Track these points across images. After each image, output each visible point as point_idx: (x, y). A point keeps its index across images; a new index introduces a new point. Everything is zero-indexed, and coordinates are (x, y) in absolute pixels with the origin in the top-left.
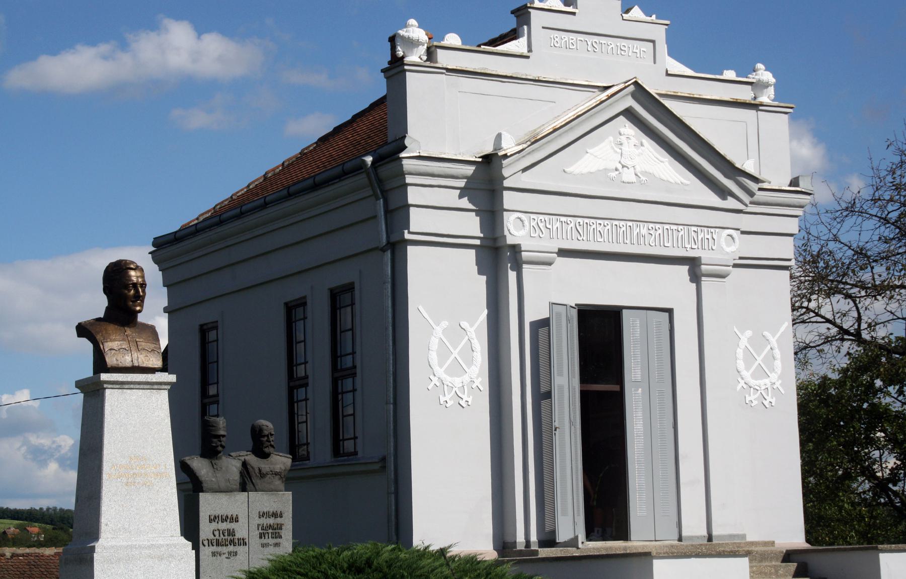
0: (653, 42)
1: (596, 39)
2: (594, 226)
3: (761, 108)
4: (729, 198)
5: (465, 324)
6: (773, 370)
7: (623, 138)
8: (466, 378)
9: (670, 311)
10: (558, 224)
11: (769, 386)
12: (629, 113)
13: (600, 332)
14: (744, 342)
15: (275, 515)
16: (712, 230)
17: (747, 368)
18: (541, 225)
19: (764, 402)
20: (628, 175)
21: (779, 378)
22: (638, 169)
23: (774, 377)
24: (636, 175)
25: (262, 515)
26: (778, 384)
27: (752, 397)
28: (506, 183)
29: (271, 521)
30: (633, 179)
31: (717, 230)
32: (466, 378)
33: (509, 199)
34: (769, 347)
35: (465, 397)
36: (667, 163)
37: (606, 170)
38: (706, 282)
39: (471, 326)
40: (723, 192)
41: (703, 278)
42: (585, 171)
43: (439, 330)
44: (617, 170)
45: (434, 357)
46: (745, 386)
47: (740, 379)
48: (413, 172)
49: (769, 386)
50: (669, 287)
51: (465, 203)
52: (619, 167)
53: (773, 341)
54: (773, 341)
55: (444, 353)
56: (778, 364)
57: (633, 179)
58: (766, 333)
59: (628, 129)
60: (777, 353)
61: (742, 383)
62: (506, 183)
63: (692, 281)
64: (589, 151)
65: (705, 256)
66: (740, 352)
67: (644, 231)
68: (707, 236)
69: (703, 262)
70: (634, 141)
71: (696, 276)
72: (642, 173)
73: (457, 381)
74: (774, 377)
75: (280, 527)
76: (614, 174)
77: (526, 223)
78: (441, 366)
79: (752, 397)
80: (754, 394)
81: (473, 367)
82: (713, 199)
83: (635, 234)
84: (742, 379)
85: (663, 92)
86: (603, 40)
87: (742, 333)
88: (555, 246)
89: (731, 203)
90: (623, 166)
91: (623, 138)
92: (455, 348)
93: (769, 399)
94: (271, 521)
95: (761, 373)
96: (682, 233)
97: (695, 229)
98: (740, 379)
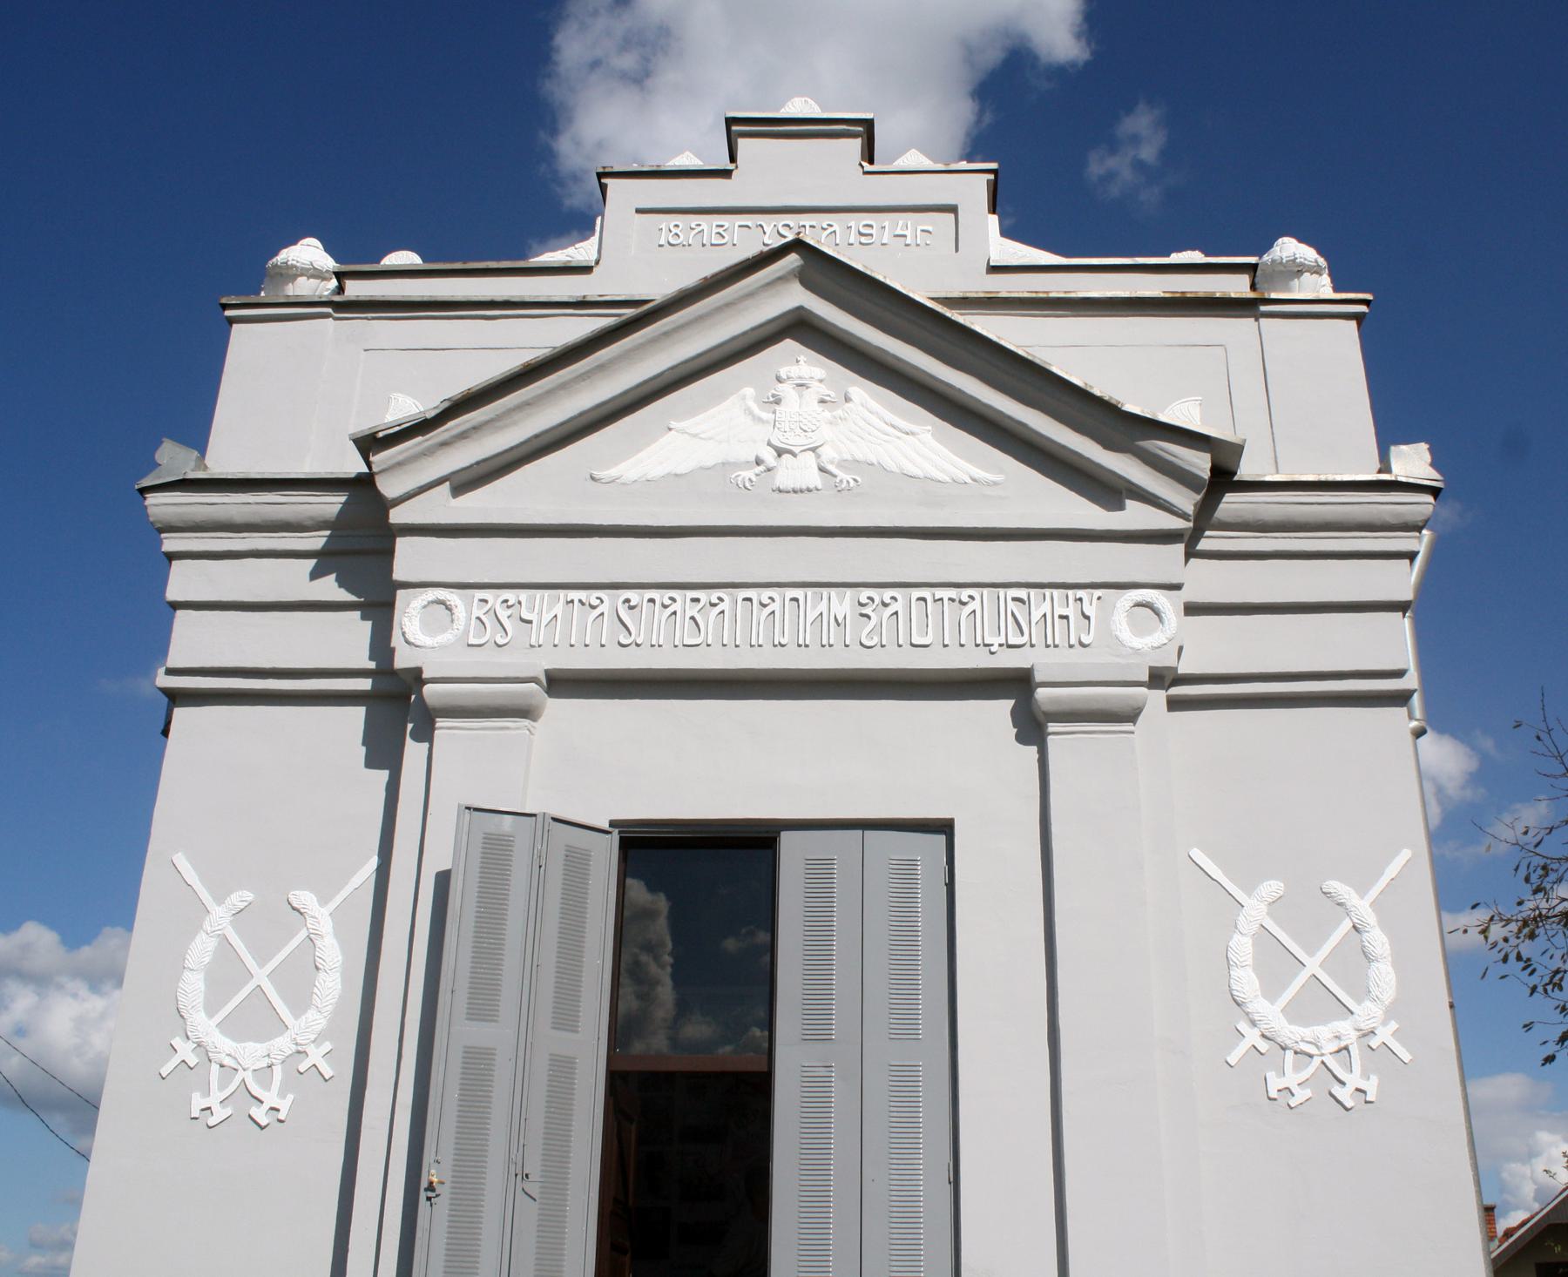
0: (953, 209)
2: (676, 607)
3: (1263, 308)
4: (1129, 503)
5: (305, 898)
7: (786, 390)
8: (282, 1045)
10: (559, 609)
11: (1351, 1038)
13: (702, 893)
14: (1255, 910)
16: (1080, 593)
17: (1271, 990)
18: (503, 614)
20: (798, 472)
21: (1390, 1013)
22: (828, 453)
23: (1368, 1013)
24: (822, 470)
26: (1385, 1034)
27: (1290, 1077)
28: (397, 516)
30: (815, 479)
31: (1098, 593)
32: (282, 1045)
33: (409, 558)
34: (1346, 925)
35: (271, 1098)
36: (928, 437)
38: (1061, 739)
39: (323, 901)
40: (1109, 491)
41: (1052, 727)
42: (656, 471)
43: (220, 916)
44: (758, 462)
45: (193, 987)
46: (1263, 1046)
47: (1243, 1026)
48: (175, 521)
49: (1351, 1038)
50: (954, 758)
51: (329, 588)
52: (769, 456)
53: (1362, 907)
54: (1362, 907)
55: (225, 974)
56: (1384, 977)
57: (815, 479)
58: (1333, 885)
60: (1377, 940)
61: (1252, 1037)
62: (397, 516)
63: (1022, 738)
64: (673, 424)
65: (1043, 663)
66: (1242, 946)
68: (1059, 611)
69: (1039, 677)
71: (1032, 727)
72: (843, 464)
73: (252, 1054)
77: (460, 612)
78: (211, 1011)
79: (1292, 1079)
80: (1297, 1068)
81: (311, 1014)
82: (1089, 514)
83: (811, 616)
84: (1253, 1023)
85: (956, 293)
87: (1249, 889)
89: (1135, 516)
90: (780, 453)
91: (786, 390)
92: (262, 963)
93: (1354, 1080)
95: (1319, 1003)
96: (975, 605)
97: (1022, 593)
98: (1243, 1026)
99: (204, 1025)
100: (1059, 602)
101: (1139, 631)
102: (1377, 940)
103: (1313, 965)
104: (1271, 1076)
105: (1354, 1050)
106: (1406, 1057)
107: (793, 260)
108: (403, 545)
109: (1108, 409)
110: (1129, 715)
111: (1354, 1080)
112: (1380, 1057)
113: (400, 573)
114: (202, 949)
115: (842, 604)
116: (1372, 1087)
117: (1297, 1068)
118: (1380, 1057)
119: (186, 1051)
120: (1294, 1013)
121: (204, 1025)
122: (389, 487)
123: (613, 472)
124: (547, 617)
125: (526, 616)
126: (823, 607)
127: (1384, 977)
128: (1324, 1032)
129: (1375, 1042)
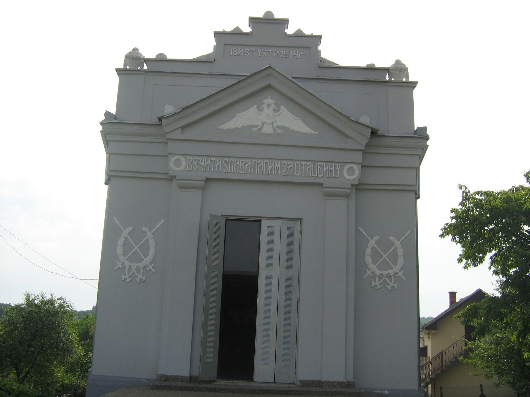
18: (195, 163)
19: (387, 286)
22: (275, 125)
23: (396, 269)
26: (400, 274)
39: (150, 230)
42: (233, 127)
56: (401, 260)
60: (400, 252)
67: (278, 166)
68: (330, 169)
69: (324, 185)
73: (134, 266)
79: (377, 283)
103: (385, 256)
104: (373, 282)
105: (393, 277)
106: (405, 279)
111: (392, 284)
116: (396, 286)
117: (379, 281)
120: (379, 268)
123: (222, 127)
124: (206, 165)
125: (200, 163)
126: (273, 165)
128: (385, 273)
129: (398, 276)
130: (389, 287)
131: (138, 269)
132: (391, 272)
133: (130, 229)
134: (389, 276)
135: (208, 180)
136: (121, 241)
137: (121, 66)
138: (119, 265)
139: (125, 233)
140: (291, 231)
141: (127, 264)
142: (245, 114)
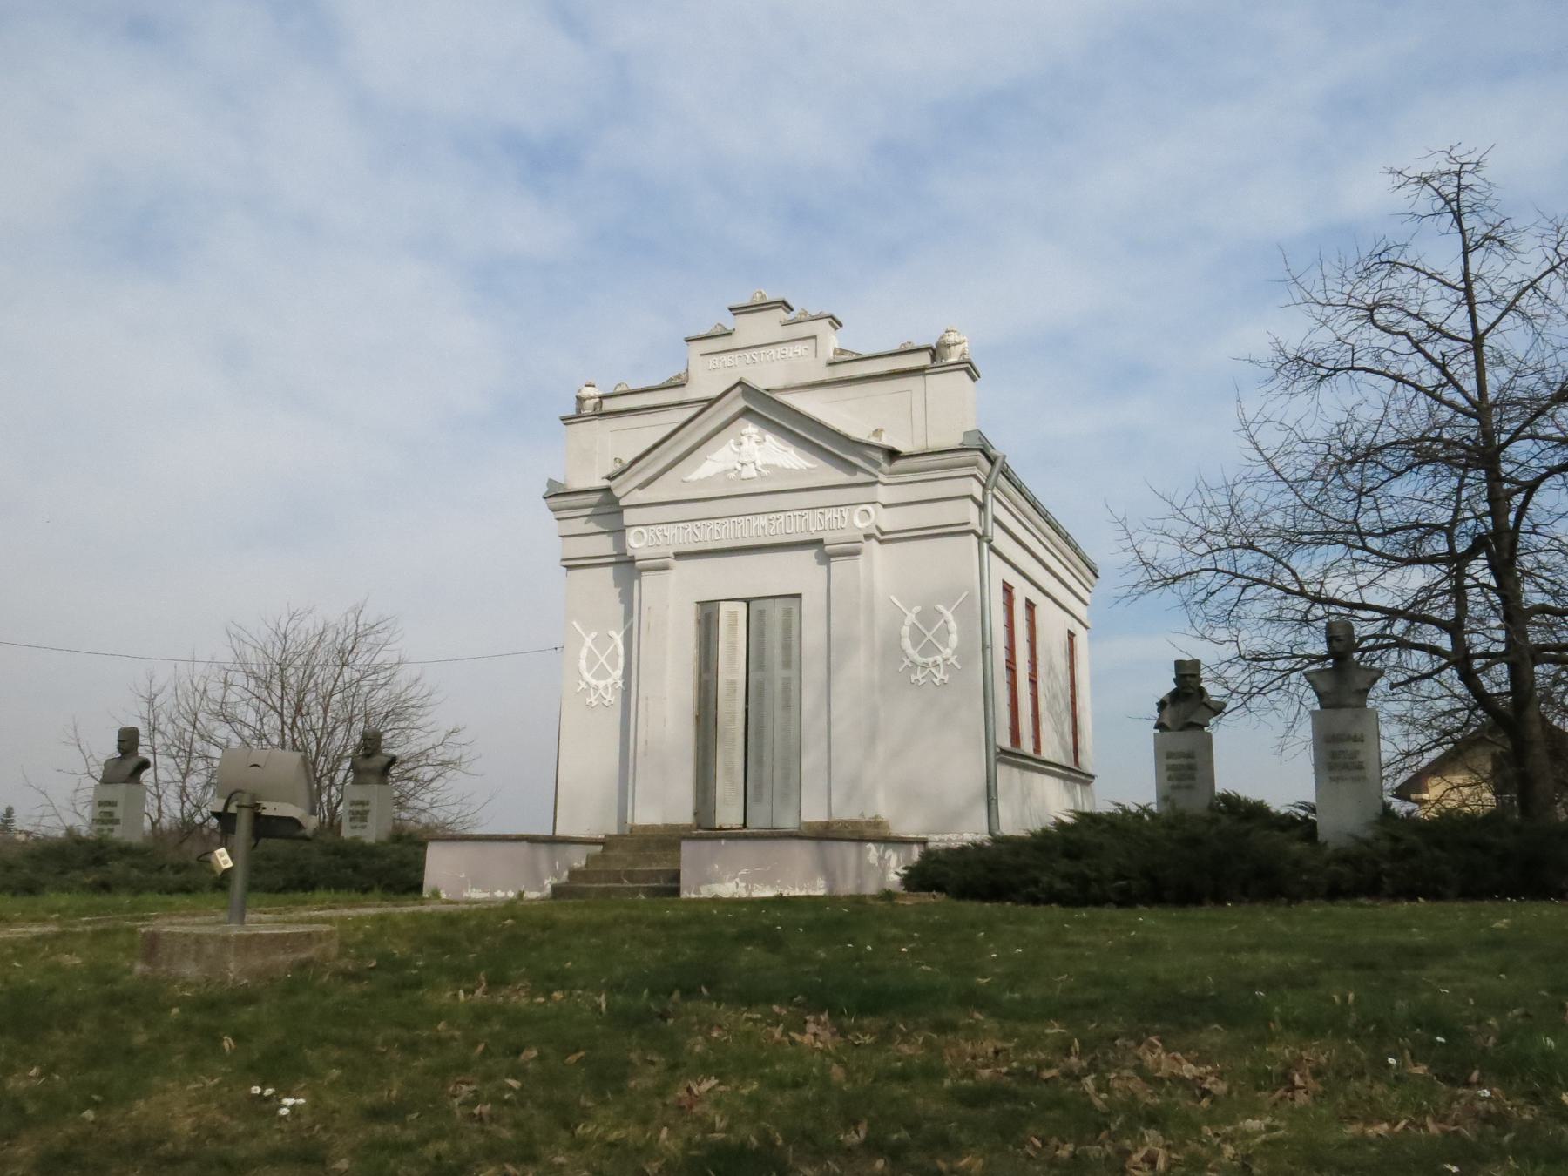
1: (756, 351)
5: (612, 633)
6: (946, 646)
7: (744, 439)
8: (610, 681)
9: (799, 596)
12: (746, 412)
15: (362, 803)
17: (915, 646)
20: (750, 472)
22: (759, 463)
25: (353, 803)
26: (952, 660)
28: (622, 503)
29: (359, 808)
30: (755, 474)
33: (629, 517)
35: (608, 697)
37: (726, 471)
40: (852, 468)
42: (703, 476)
43: (588, 642)
45: (583, 664)
54: (949, 615)
55: (592, 660)
57: (755, 474)
58: (941, 607)
59: (751, 429)
60: (953, 626)
61: (907, 662)
62: (622, 503)
63: (820, 563)
65: (827, 537)
70: (756, 437)
71: (826, 558)
72: (766, 466)
73: (601, 684)
74: (948, 652)
75: (367, 812)
76: (732, 475)
79: (919, 676)
86: (762, 350)
88: (671, 552)
89: (861, 477)
91: (744, 439)
94: (359, 808)
99: (587, 676)
100: (833, 513)
101: (862, 520)
102: (953, 626)
107: (739, 389)
108: (626, 512)
109: (846, 438)
110: (856, 553)
111: (940, 676)
112: (949, 668)
113: (626, 522)
114: (584, 653)
115: (763, 520)
116: (946, 678)
118: (949, 668)
119: (583, 685)
120: (923, 653)
121: (587, 676)
122: (617, 493)
127: (954, 639)
128: (930, 660)
130: (937, 681)
131: (606, 688)
132: (939, 659)
133: (594, 635)
134: (936, 665)
135: (679, 556)
136: (584, 653)
137: (573, 412)
138: (583, 685)
139: (588, 642)
140: (788, 613)
141: (593, 682)
142: (715, 456)
